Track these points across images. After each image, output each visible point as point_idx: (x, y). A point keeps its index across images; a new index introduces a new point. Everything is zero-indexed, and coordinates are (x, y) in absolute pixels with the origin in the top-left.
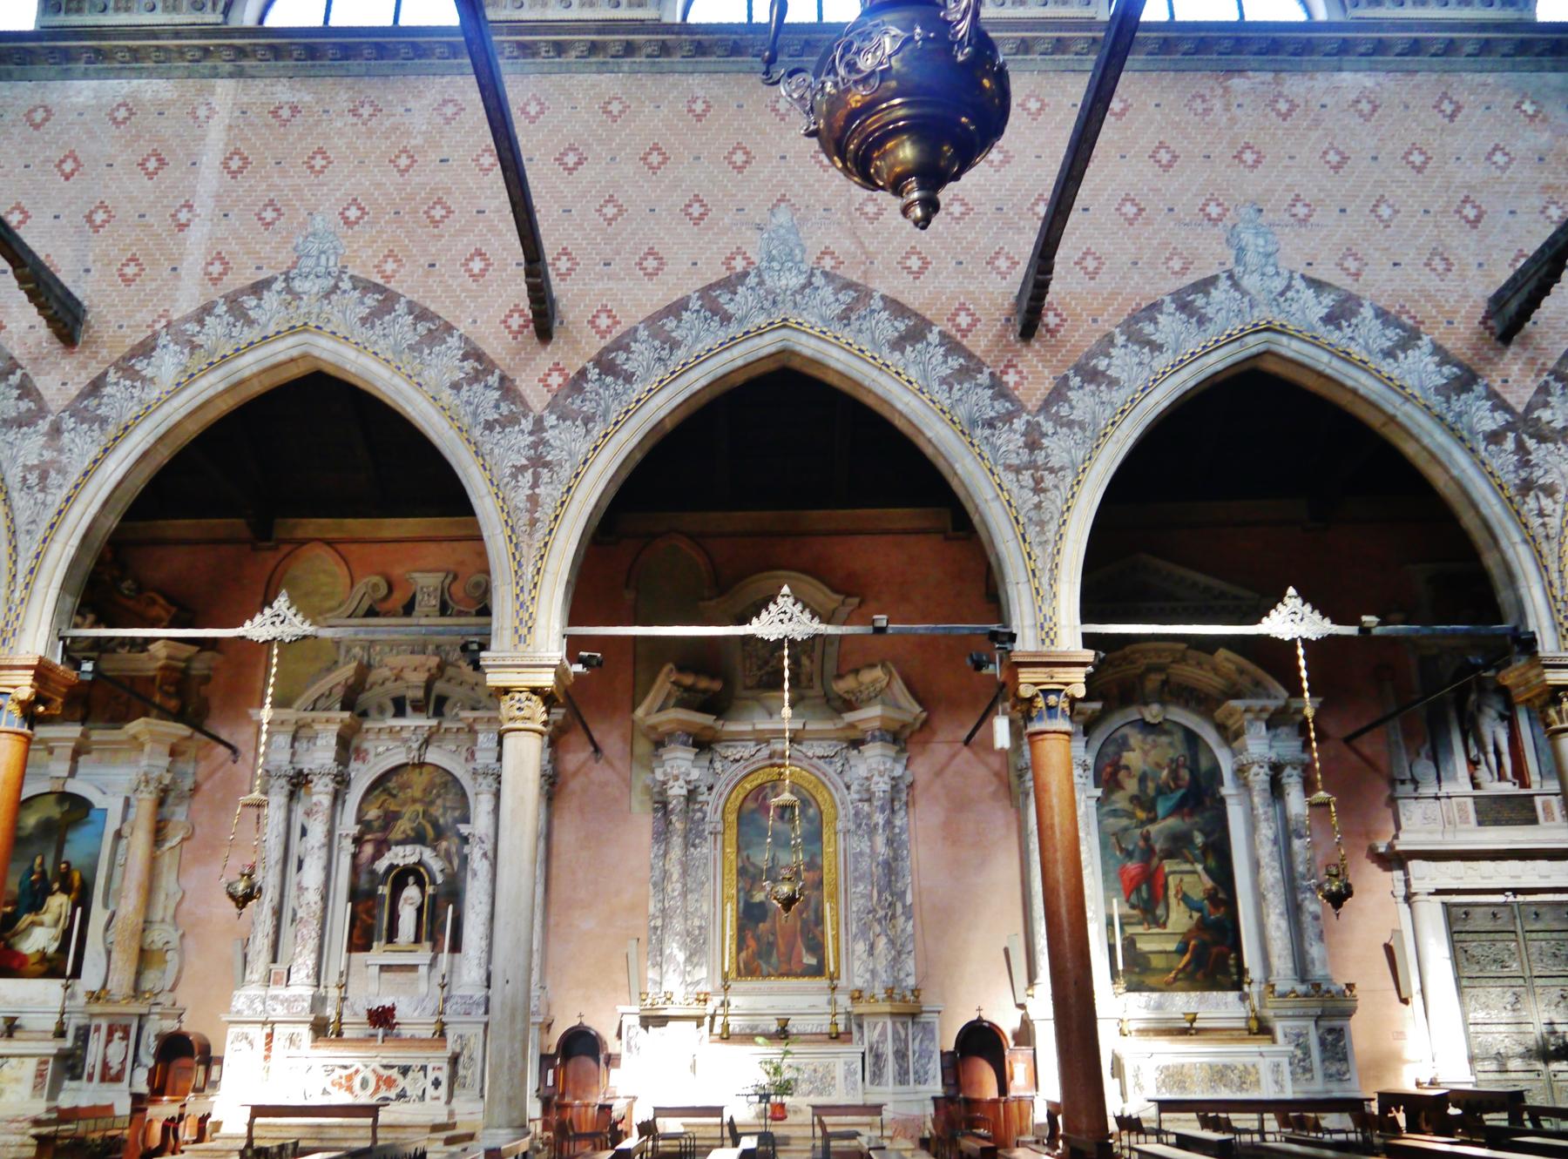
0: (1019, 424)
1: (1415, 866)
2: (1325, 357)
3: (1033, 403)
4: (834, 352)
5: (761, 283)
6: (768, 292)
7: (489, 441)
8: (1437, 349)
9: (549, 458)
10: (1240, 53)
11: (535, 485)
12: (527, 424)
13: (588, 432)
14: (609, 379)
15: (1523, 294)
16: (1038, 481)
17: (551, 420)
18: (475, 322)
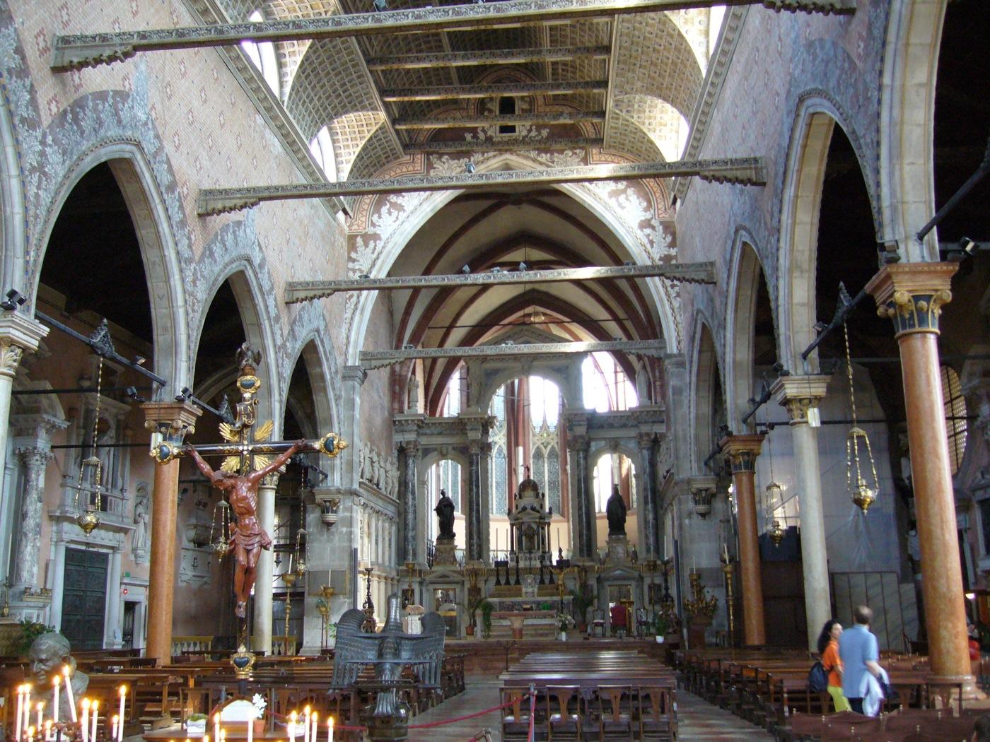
0: (193, 265)
1: (66, 526)
2: (255, 283)
3: (197, 258)
4: (147, 175)
5: (133, 107)
6: (135, 117)
7: (23, 132)
8: (275, 300)
9: (46, 170)
10: (261, 102)
11: (39, 187)
12: (39, 133)
13: (64, 161)
14: (75, 128)
15: (311, 294)
16: (194, 304)
17: (49, 140)
18: (23, 23)
